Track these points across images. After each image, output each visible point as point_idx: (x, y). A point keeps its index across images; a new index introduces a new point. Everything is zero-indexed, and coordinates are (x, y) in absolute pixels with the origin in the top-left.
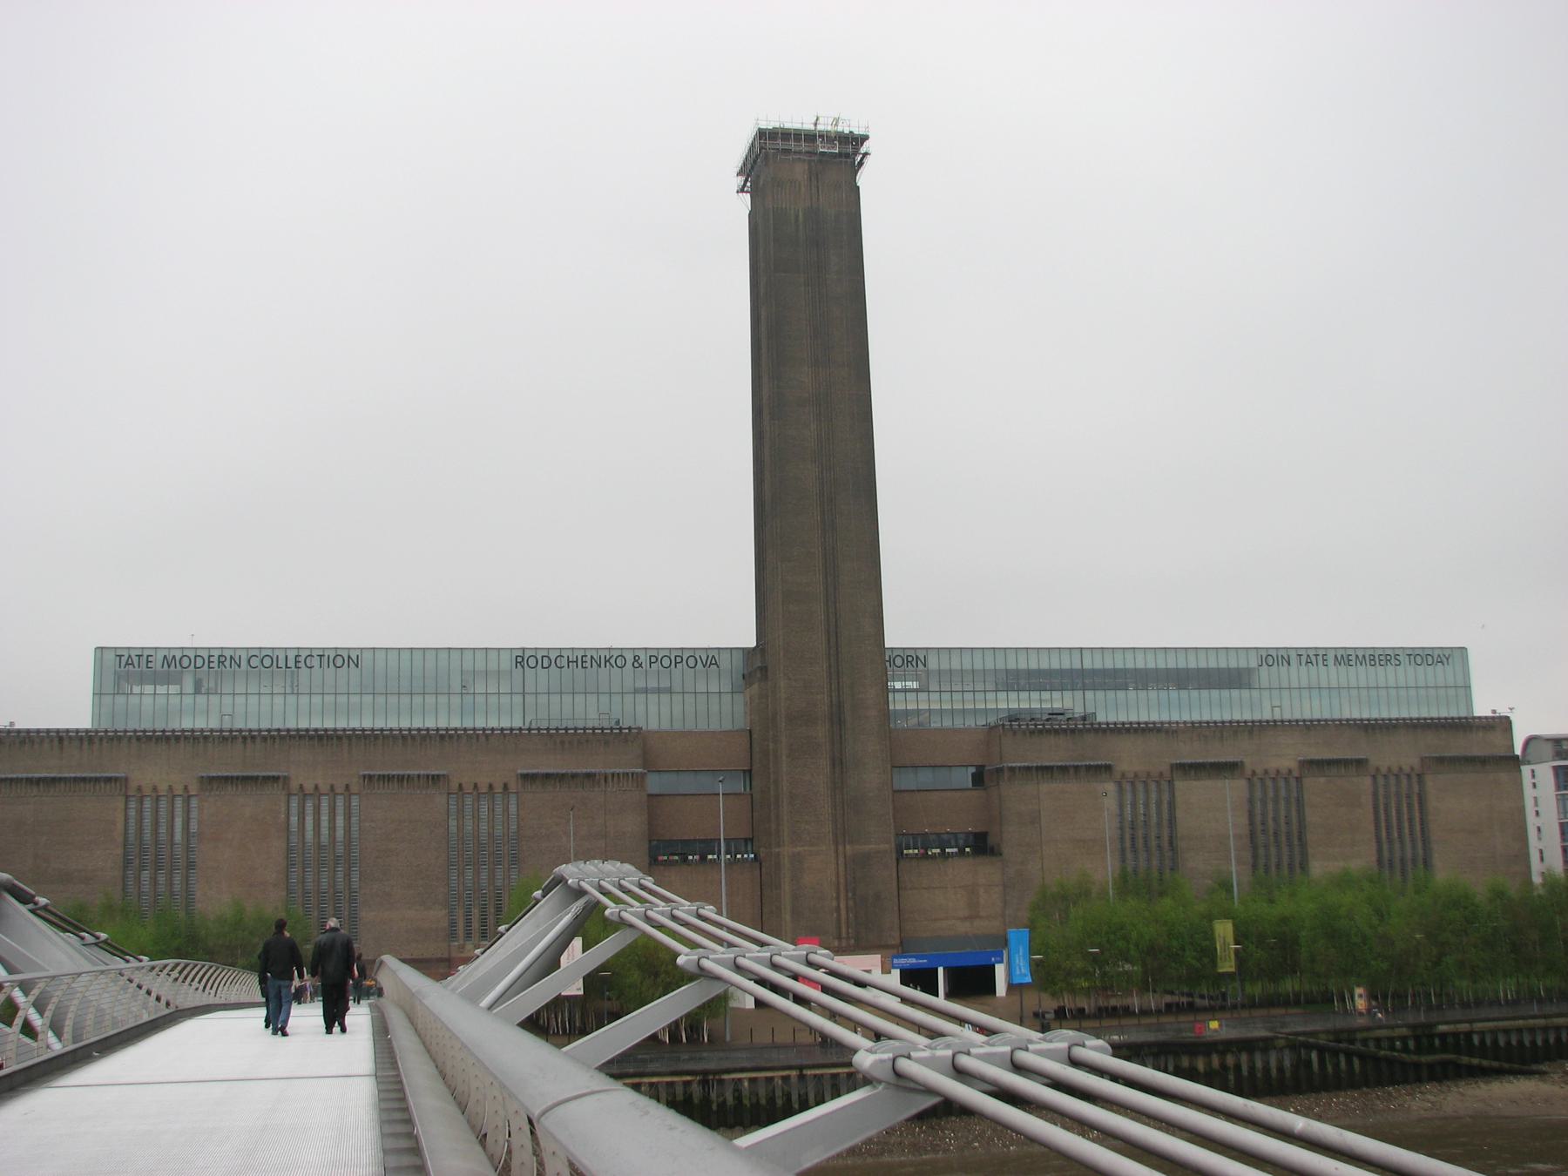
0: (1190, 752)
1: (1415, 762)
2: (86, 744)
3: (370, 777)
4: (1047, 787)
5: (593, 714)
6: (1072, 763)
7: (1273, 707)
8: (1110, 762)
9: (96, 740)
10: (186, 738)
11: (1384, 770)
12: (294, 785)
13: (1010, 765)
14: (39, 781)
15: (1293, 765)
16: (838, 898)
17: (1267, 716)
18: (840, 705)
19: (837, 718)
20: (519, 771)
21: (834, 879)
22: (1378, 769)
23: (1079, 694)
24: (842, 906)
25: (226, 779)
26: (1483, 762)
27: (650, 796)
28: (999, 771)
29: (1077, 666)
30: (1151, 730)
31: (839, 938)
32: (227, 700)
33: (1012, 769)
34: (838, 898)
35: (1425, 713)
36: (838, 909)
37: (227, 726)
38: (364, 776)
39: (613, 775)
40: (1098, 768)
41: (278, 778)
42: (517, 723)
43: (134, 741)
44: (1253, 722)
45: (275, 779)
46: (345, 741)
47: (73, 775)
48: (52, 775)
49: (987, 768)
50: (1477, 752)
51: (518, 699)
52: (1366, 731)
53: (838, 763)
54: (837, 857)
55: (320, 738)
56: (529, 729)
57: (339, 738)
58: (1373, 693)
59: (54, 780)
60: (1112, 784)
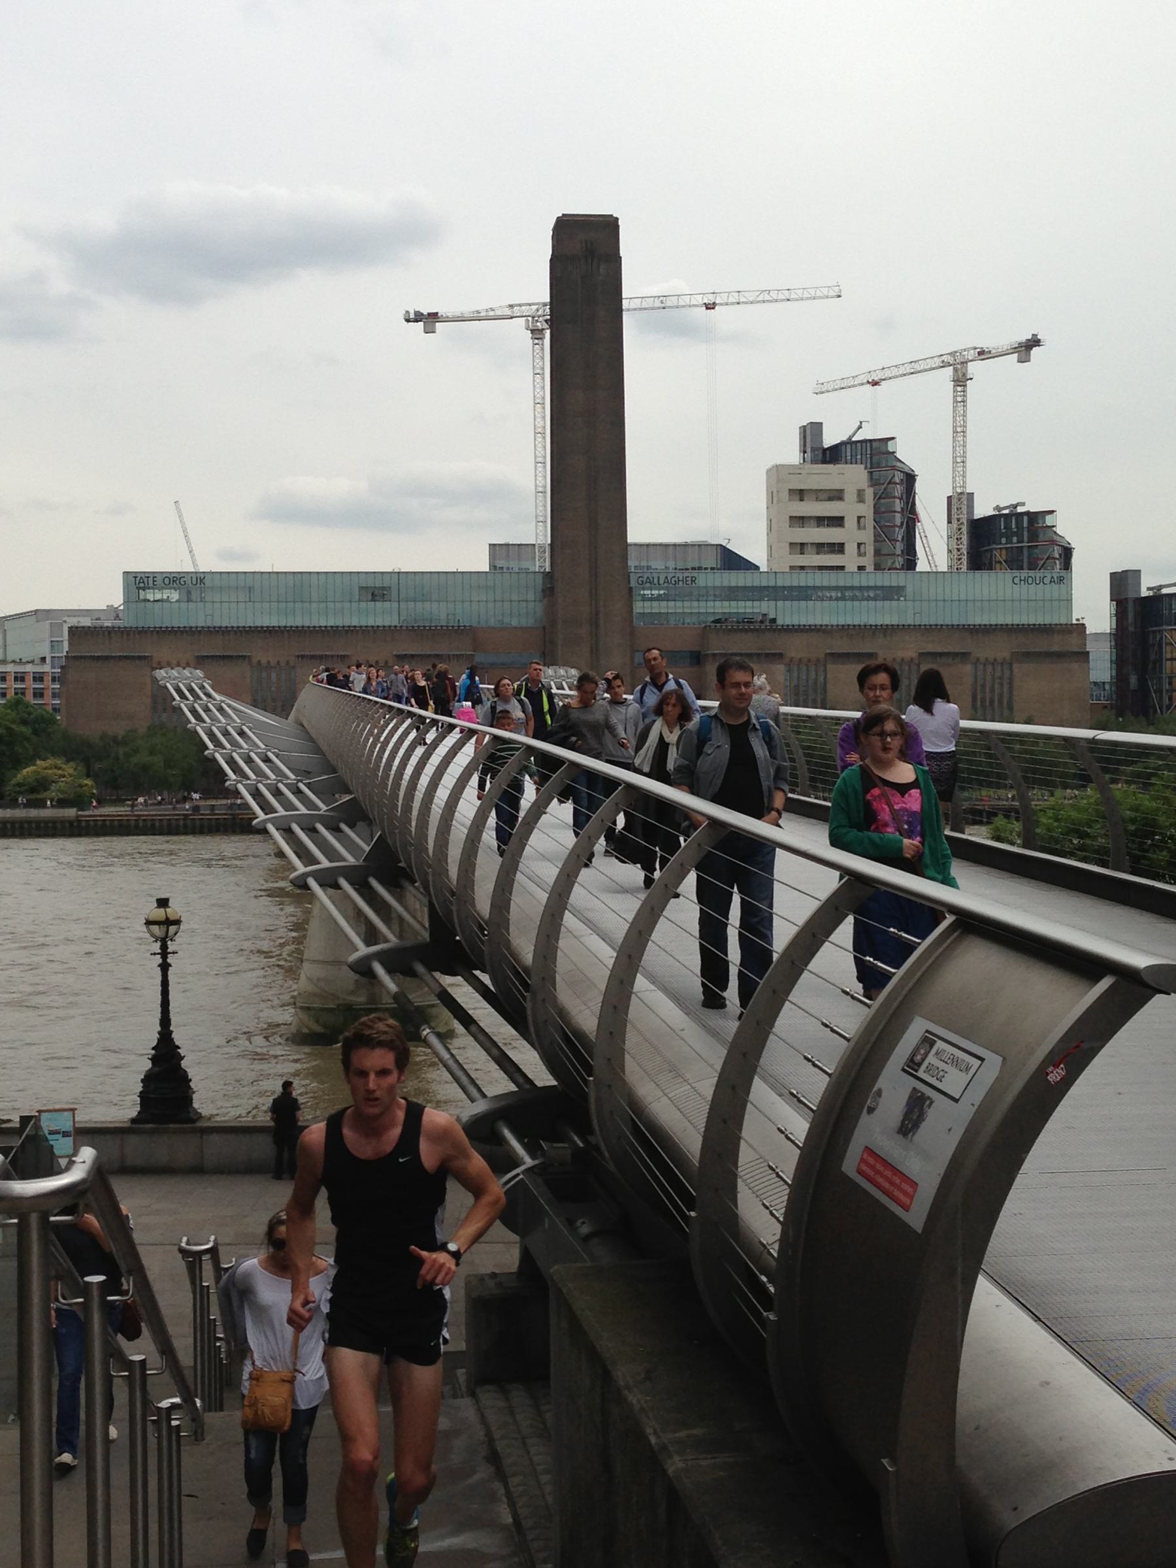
0: (841, 645)
1: (1007, 655)
2: (125, 636)
3: (303, 657)
5: (443, 616)
6: (755, 651)
7: (914, 614)
8: (781, 651)
9: (132, 633)
10: (187, 631)
11: (982, 660)
12: (254, 661)
13: (713, 652)
14: (98, 658)
15: (914, 655)
17: (910, 621)
18: (597, 613)
19: (594, 623)
20: (394, 653)
22: (978, 659)
23: (772, 603)
25: (212, 656)
26: (1060, 656)
28: (707, 655)
29: (772, 584)
30: (812, 630)
32: (209, 605)
33: (714, 655)
35: (1017, 620)
37: (209, 624)
38: (298, 656)
39: (453, 655)
40: (774, 655)
41: (245, 656)
42: (395, 622)
43: (155, 633)
44: (876, 626)
45: (244, 657)
46: (286, 634)
47: (118, 654)
48: (106, 654)
50: (1055, 648)
51: (395, 605)
52: (971, 633)
55: (270, 632)
56: (401, 627)
57: (282, 632)
58: (1056, 604)
59: (107, 658)
60: (783, 666)
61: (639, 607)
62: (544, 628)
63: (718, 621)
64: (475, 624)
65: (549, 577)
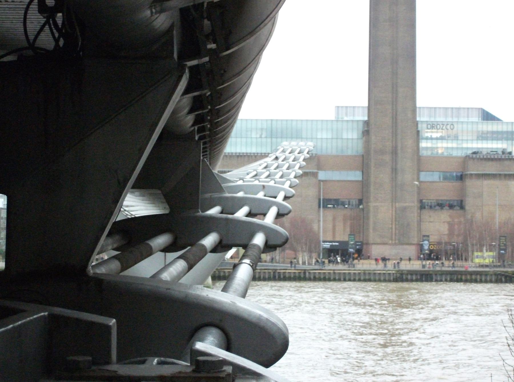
4: (487, 183)
16: (392, 224)
19: (394, 152)
21: (391, 217)
24: (394, 226)
27: (320, 181)
31: (392, 240)
33: (471, 175)
34: (392, 224)
36: (392, 228)
49: (464, 173)
53: (395, 171)
54: (392, 208)
61: (423, 144)
62: (363, 156)
63: (474, 153)
64: (319, 153)
65: (367, 123)
